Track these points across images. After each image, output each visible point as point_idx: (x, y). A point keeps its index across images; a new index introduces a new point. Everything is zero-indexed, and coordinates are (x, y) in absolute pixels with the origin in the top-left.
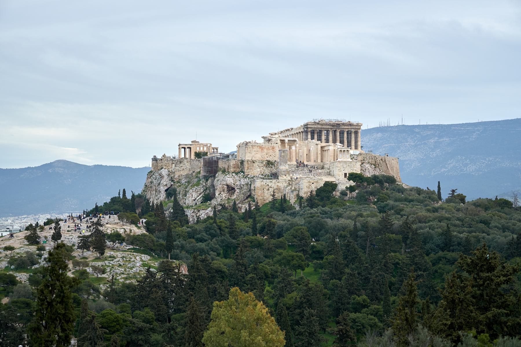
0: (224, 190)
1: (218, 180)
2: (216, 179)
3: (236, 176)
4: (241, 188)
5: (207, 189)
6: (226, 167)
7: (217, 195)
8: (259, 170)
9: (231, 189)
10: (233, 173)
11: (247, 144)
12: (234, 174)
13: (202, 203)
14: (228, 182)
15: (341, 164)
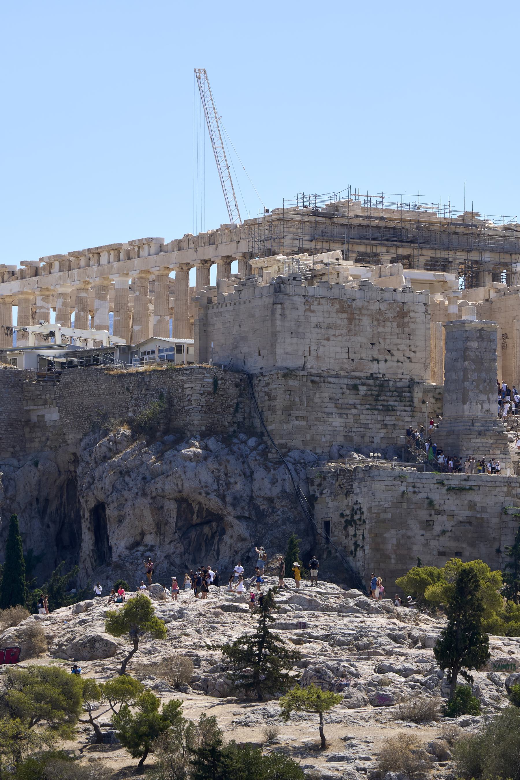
4: (261, 515)
8: (337, 423)
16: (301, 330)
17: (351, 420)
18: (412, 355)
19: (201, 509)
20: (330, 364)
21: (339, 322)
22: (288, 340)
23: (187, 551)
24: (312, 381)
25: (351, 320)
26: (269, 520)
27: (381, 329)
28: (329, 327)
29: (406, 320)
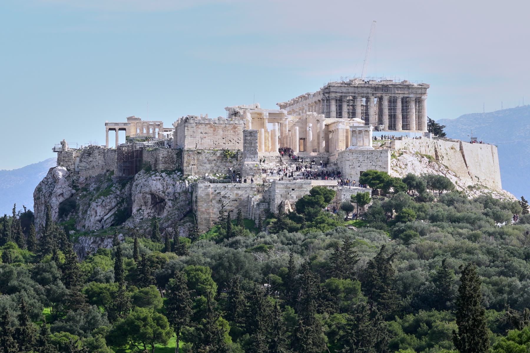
0: (146, 203)
1: (137, 185)
2: (135, 183)
3: (166, 178)
4: (176, 198)
5: (123, 201)
6: (152, 161)
7: (134, 210)
8: (208, 166)
9: (158, 202)
10: (162, 172)
11: (186, 120)
12: (164, 174)
13: (112, 225)
14: (154, 189)
15: (355, 156)
16: (195, 135)
17: (213, 165)
18: (239, 141)
19: (159, 197)
20: (206, 146)
21: (210, 131)
22: (190, 138)
23: (155, 211)
24: (198, 152)
25: (214, 131)
26: (178, 201)
27: (226, 133)
28: (206, 133)
29: (236, 129)
